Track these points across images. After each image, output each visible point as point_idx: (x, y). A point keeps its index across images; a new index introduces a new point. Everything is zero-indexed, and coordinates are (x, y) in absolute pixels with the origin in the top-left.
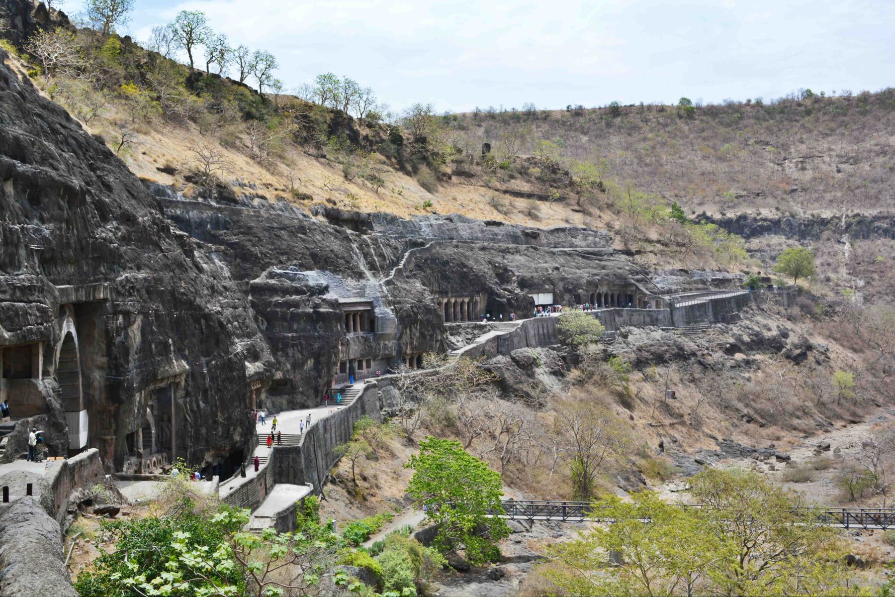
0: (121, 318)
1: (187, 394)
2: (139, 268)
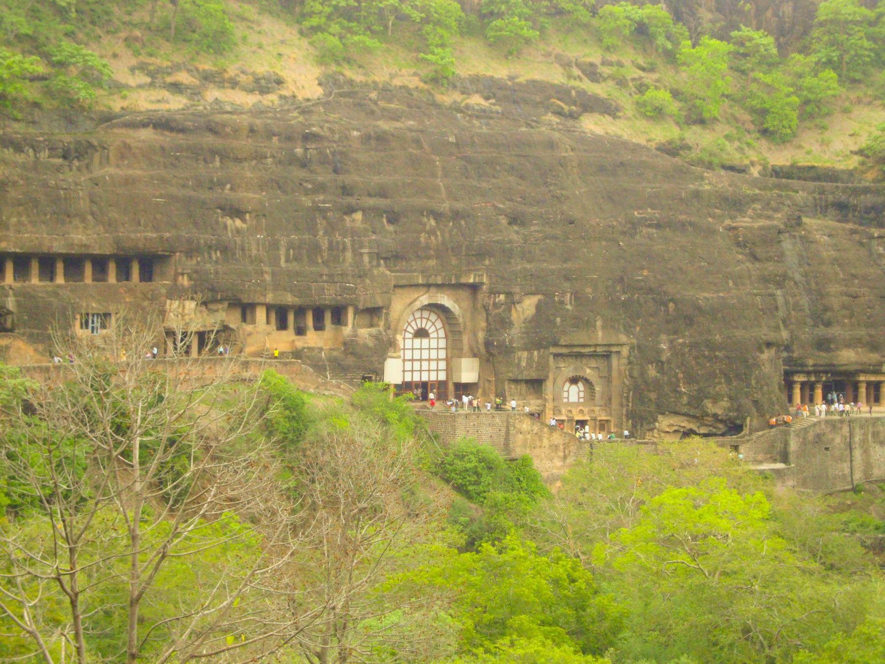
0: (502, 297)
1: (630, 363)
2: (565, 262)
